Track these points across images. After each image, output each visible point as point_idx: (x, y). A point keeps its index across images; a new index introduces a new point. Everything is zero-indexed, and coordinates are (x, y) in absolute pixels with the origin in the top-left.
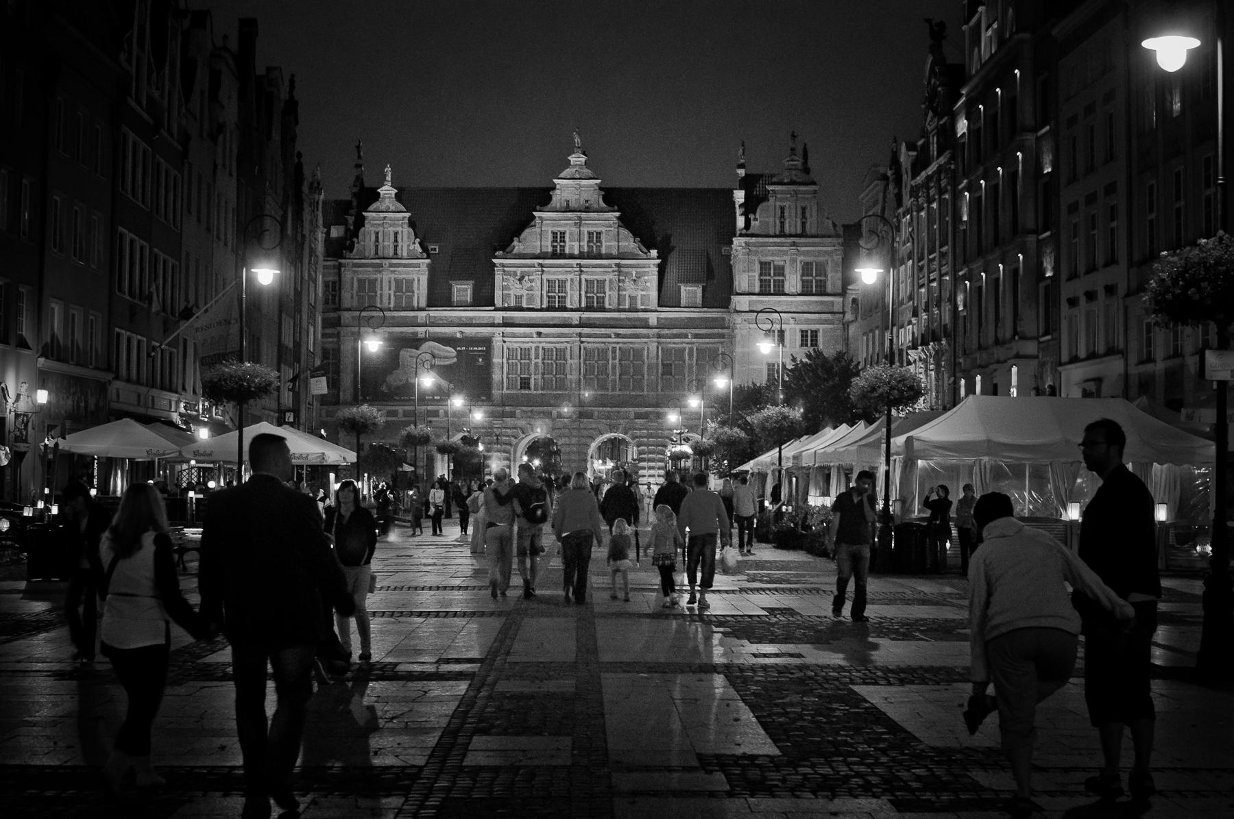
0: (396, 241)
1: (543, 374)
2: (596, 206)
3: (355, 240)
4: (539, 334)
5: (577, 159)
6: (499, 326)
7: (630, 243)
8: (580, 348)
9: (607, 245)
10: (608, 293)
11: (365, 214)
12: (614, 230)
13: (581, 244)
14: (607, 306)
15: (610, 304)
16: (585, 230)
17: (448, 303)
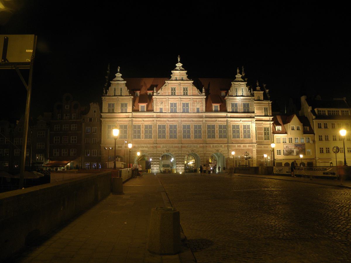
0: (121, 91)
1: (170, 133)
2: (185, 79)
3: (108, 90)
4: (168, 121)
5: (179, 65)
6: (155, 118)
7: (196, 91)
8: (181, 125)
9: (190, 92)
10: (190, 107)
11: (111, 82)
12: (191, 87)
13: (181, 91)
14: (190, 112)
15: (190, 111)
16: (182, 87)
17: (138, 111)
